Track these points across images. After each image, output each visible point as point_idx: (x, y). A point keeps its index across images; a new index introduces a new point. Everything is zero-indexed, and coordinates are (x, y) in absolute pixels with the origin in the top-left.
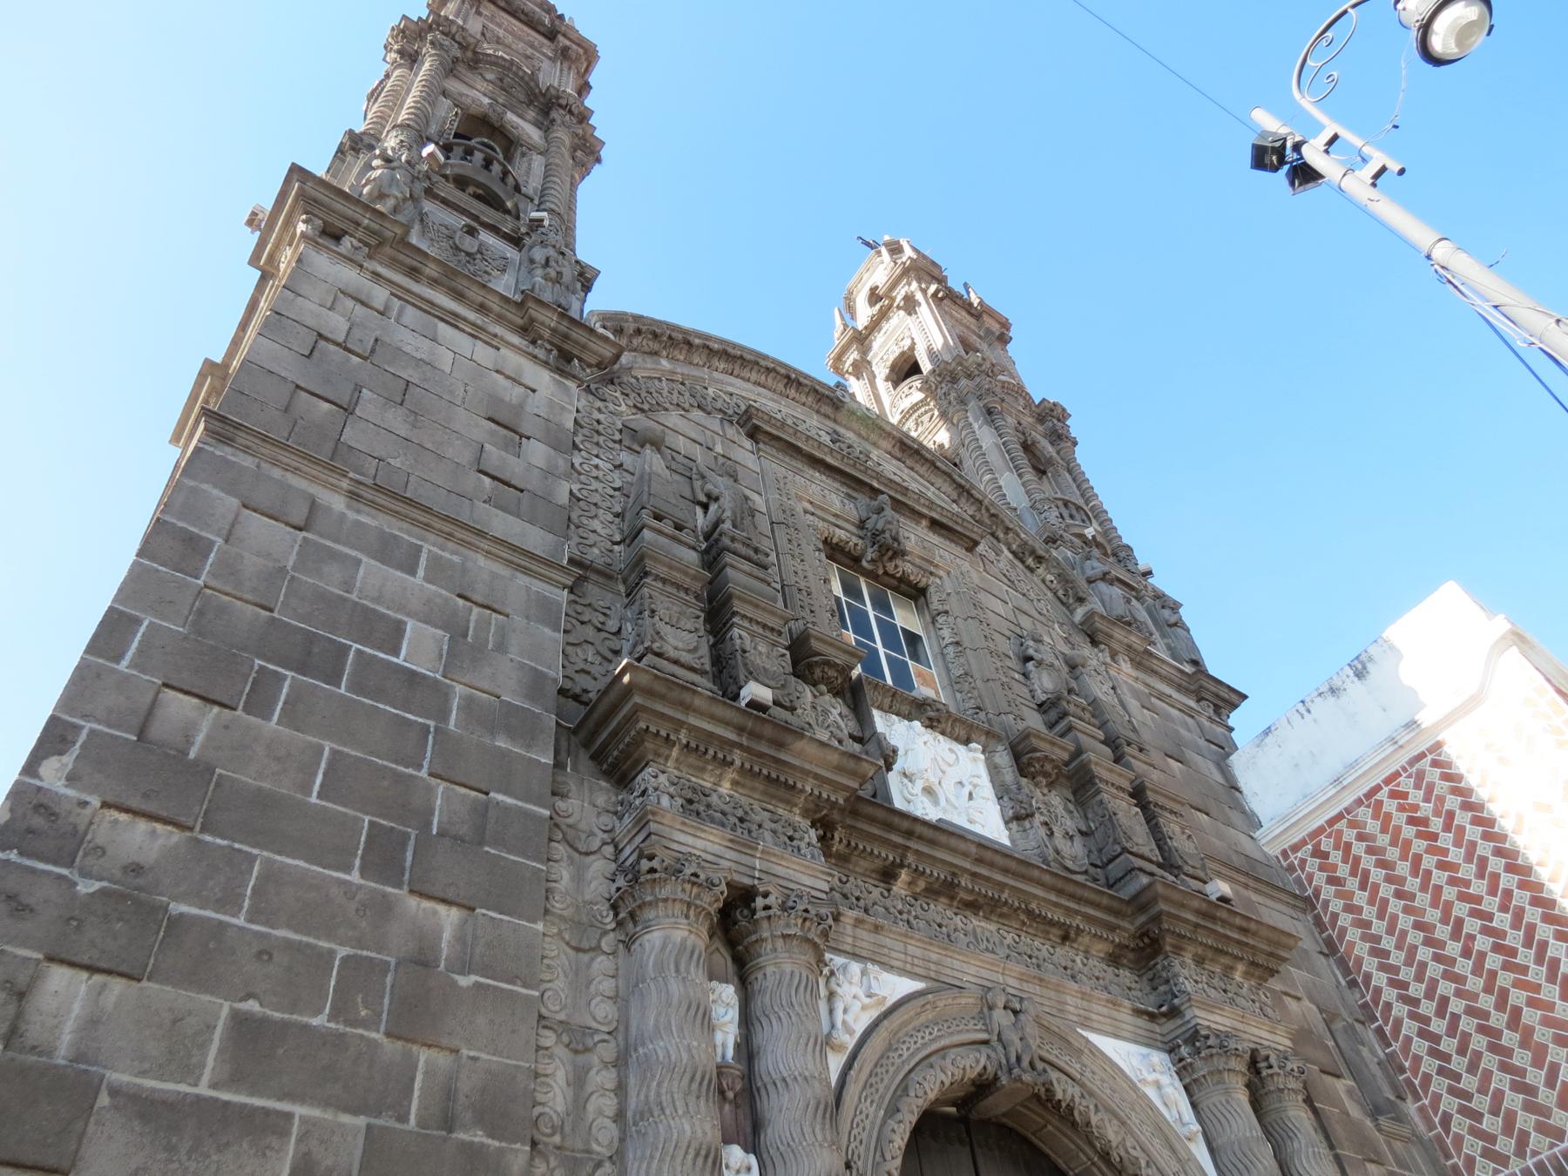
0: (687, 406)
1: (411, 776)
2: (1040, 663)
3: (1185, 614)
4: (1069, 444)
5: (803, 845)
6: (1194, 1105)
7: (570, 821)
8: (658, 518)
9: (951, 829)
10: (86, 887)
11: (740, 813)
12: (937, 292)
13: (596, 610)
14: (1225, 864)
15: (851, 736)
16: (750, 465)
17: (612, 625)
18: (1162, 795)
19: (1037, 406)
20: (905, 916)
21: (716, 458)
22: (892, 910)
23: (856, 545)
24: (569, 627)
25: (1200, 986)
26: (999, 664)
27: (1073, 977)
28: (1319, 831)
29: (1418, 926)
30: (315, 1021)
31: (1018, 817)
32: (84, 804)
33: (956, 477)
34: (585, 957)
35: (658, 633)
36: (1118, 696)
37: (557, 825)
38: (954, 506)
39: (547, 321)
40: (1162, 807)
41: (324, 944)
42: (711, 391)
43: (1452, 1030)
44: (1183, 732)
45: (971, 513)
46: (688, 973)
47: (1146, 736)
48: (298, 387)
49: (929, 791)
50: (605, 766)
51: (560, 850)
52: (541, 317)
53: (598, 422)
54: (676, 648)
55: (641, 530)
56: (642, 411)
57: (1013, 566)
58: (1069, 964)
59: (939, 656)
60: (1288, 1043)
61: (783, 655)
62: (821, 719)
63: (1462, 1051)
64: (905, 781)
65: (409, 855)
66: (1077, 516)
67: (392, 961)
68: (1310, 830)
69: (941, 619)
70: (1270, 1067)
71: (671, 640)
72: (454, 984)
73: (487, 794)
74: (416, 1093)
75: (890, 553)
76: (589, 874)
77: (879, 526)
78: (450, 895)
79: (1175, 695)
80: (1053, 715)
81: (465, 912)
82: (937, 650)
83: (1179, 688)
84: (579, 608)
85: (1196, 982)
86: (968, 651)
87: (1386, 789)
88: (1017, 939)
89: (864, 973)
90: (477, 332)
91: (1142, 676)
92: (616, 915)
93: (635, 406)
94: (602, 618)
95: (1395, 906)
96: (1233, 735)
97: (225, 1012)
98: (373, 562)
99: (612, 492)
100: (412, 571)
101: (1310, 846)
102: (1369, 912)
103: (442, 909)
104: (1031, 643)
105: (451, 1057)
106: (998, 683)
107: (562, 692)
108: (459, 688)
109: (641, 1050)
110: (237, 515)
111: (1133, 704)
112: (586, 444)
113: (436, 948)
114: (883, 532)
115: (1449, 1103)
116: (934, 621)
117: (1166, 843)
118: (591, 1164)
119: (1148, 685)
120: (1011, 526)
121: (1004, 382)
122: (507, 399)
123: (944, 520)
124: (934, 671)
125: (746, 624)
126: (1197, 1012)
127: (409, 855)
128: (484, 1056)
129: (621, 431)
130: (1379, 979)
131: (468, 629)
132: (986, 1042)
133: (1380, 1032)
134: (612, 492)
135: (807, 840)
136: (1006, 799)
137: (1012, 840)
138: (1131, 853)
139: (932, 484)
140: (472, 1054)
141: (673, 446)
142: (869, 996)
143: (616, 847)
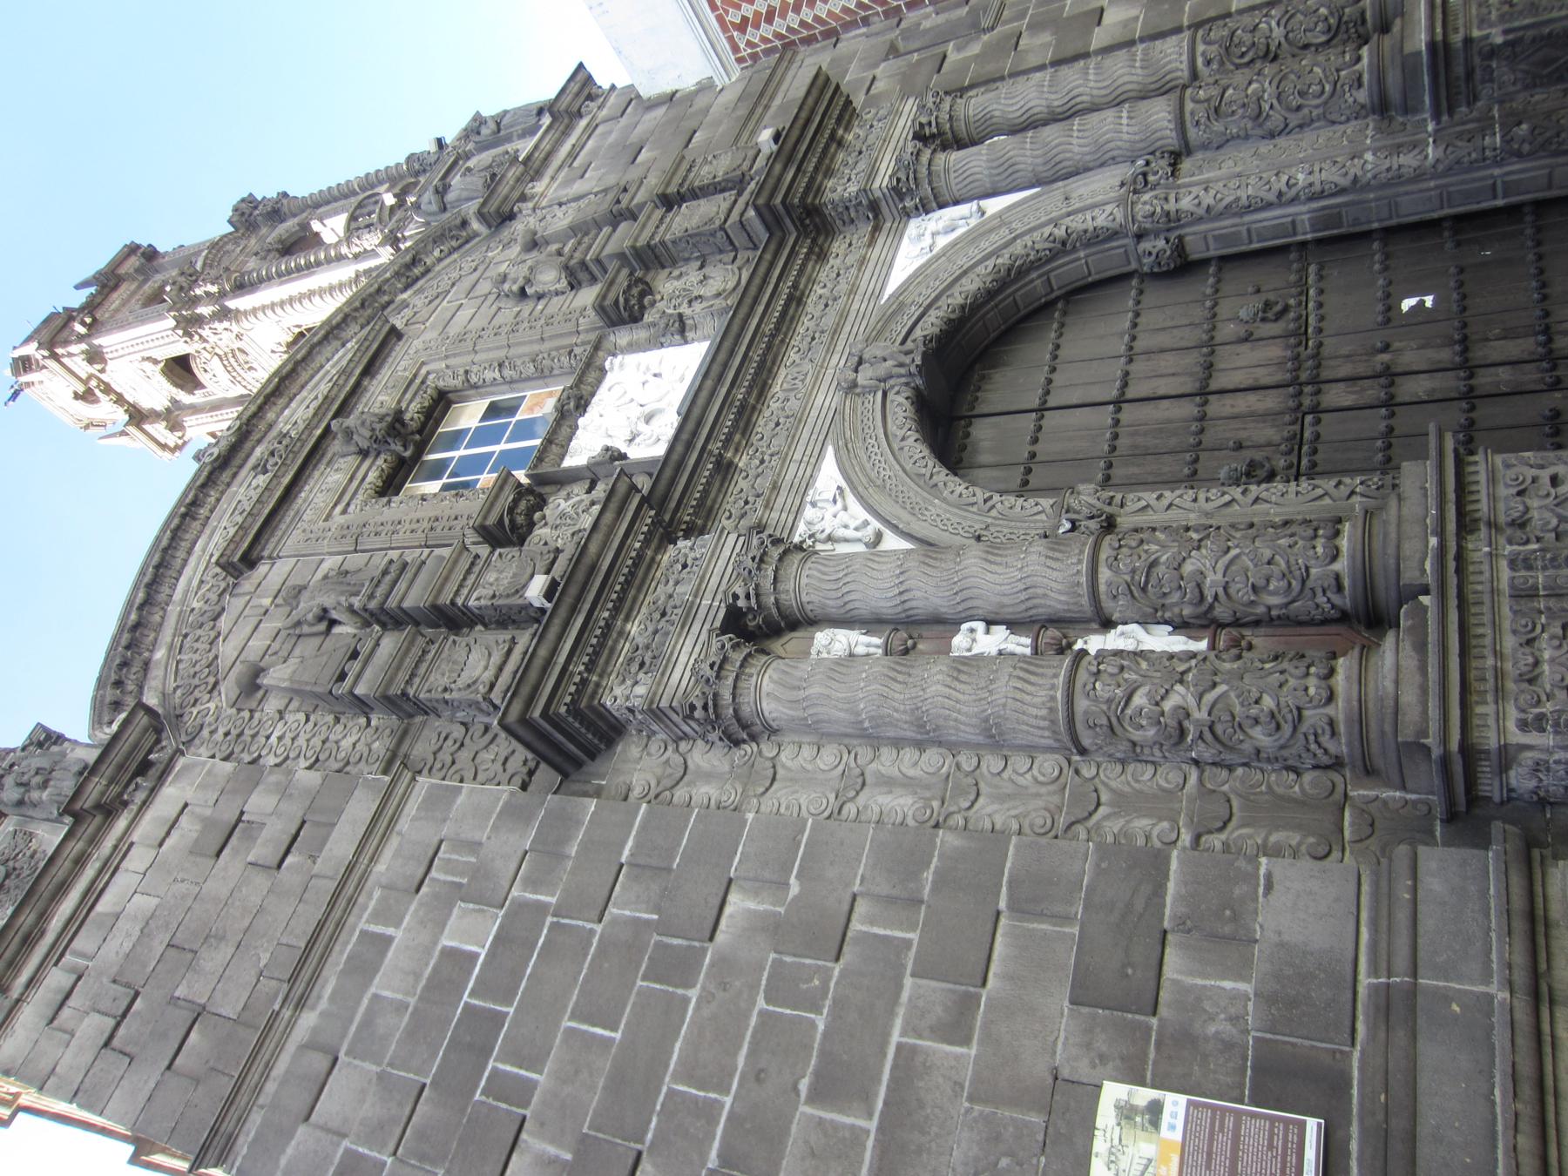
0: (213, 634)
1: (600, 940)
2: (528, 281)
3: (489, 111)
4: (285, 201)
5: (692, 555)
6: (956, 203)
7: (653, 784)
8: (342, 677)
9: (688, 403)
11: (657, 616)
12: (83, 323)
13: (441, 748)
14: (745, 125)
15: (589, 491)
16: (288, 568)
17: (458, 731)
18: (671, 178)
19: (237, 231)
20: (767, 458)
21: (276, 606)
22: (760, 470)
23: (385, 461)
24: (457, 777)
25: (853, 177)
26: (526, 324)
27: (835, 299)
28: (720, 19)
30: (821, 1027)
31: (681, 329)
33: (316, 339)
34: (781, 772)
35: (469, 686)
36: (569, 201)
37: (657, 797)
38: (349, 345)
39: (99, 788)
40: (684, 180)
41: (753, 1020)
42: (195, 605)
44: (612, 139)
45: (357, 328)
46: (801, 679)
47: (611, 180)
48: (169, 1067)
49: (648, 419)
50: (602, 746)
51: (680, 794)
52: (94, 796)
53: (227, 734)
54: (486, 668)
55: (356, 697)
56: (216, 684)
57: (421, 291)
58: (823, 301)
59: (514, 386)
60: (911, 101)
61: (500, 555)
62: (568, 521)
64: (637, 440)
65: (676, 941)
66: (370, 208)
67: (773, 956)
68: (719, 30)
69: (474, 379)
70: (930, 124)
71: (477, 673)
72: (796, 898)
73: (622, 866)
74: (888, 932)
75: (397, 426)
76: (705, 765)
77: (368, 434)
78: (717, 902)
79: (572, 140)
80: (583, 276)
81: (733, 887)
82: (505, 387)
83: (566, 133)
84: (438, 765)
85: (849, 180)
86: (510, 355)
88: (796, 349)
90: (110, 868)
91: (550, 172)
92: (744, 741)
93: (210, 692)
94: (450, 742)
96: (619, 86)
97: (808, 1110)
98: (377, 980)
99: (311, 724)
100: (389, 940)
101: (735, 34)
104: (506, 287)
105: (859, 901)
106: (546, 328)
107: (524, 787)
108: (515, 893)
109: (866, 724)
110: (318, 1127)
111: (578, 187)
112: (253, 748)
113: (765, 915)
114: (373, 430)
116: (475, 387)
117: (719, 183)
118: (958, 773)
119: (560, 168)
120: (376, 286)
121: (204, 264)
122: (195, 835)
123: (365, 360)
124: (528, 394)
125: (465, 591)
126: (876, 185)
127: (676, 941)
128: (860, 872)
129: (239, 710)
131: (453, 883)
132: (885, 394)
134: (311, 724)
135: (687, 551)
136: (663, 340)
137: (705, 338)
138: (726, 221)
139: (322, 367)
140: (858, 881)
141: (261, 653)
142: (835, 501)
143: (681, 739)
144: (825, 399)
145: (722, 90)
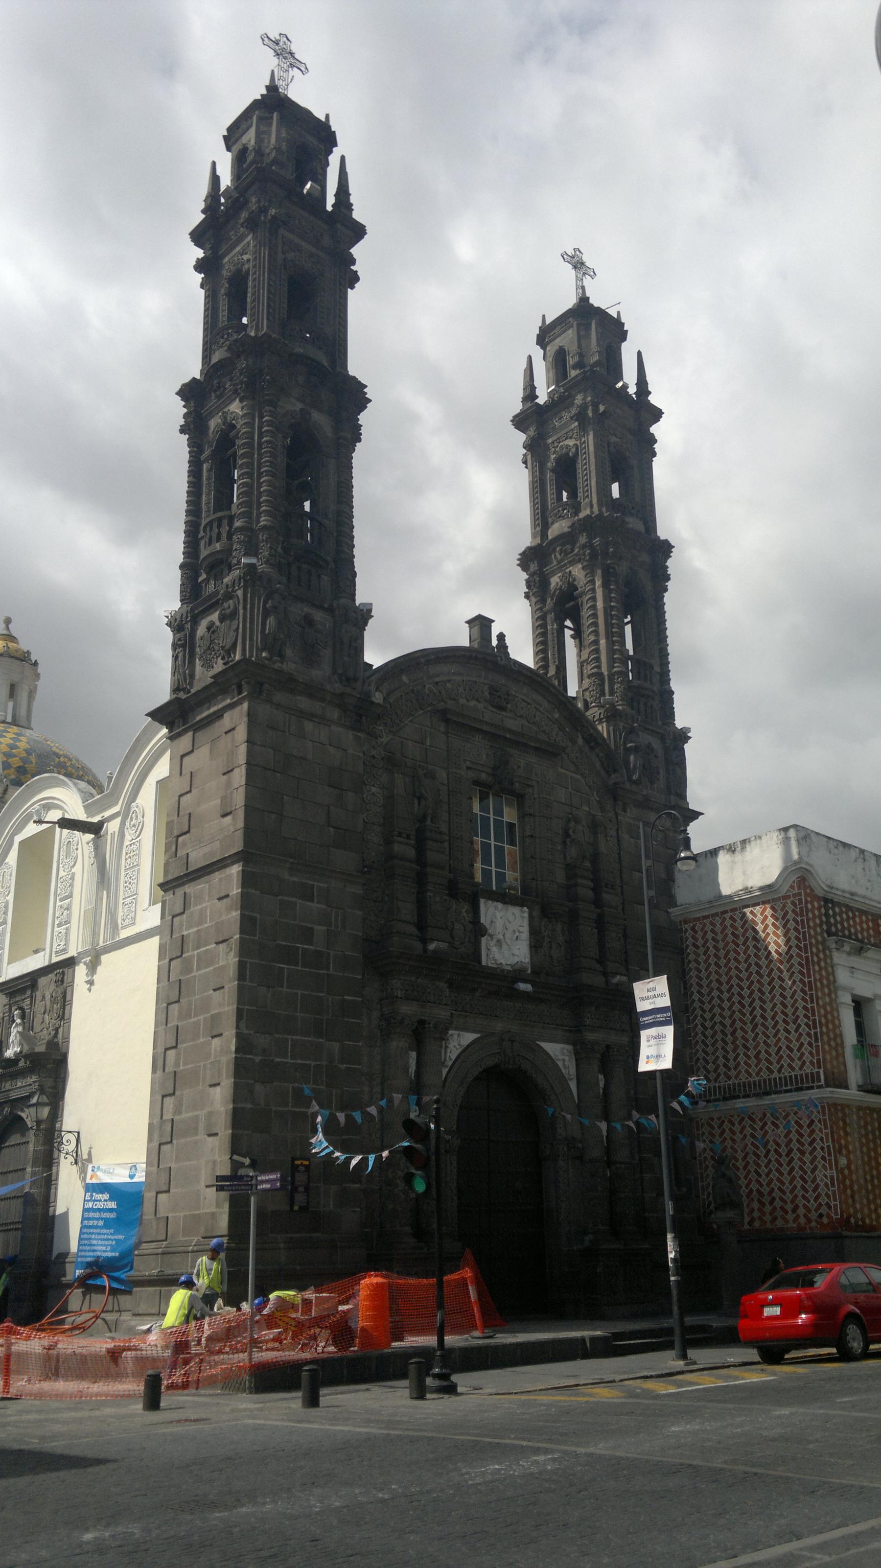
8: (400, 835)
10: (258, 1059)
15: (470, 922)
28: (698, 919)
29: (718, 981)
32: (251, 1034)
43: (712, 1027)
53: (373, 757)
63: (712, 1037)
87: (729, 914)
89: (459, 1035)
95: (713, 968)
101: (691, 925)
102: (702, 966)
103: (334, 1043)
115: (701, 1055)
130: (696, 996)
133: (688, 1017)
144: (499, 1026)
145: (667, 912)
